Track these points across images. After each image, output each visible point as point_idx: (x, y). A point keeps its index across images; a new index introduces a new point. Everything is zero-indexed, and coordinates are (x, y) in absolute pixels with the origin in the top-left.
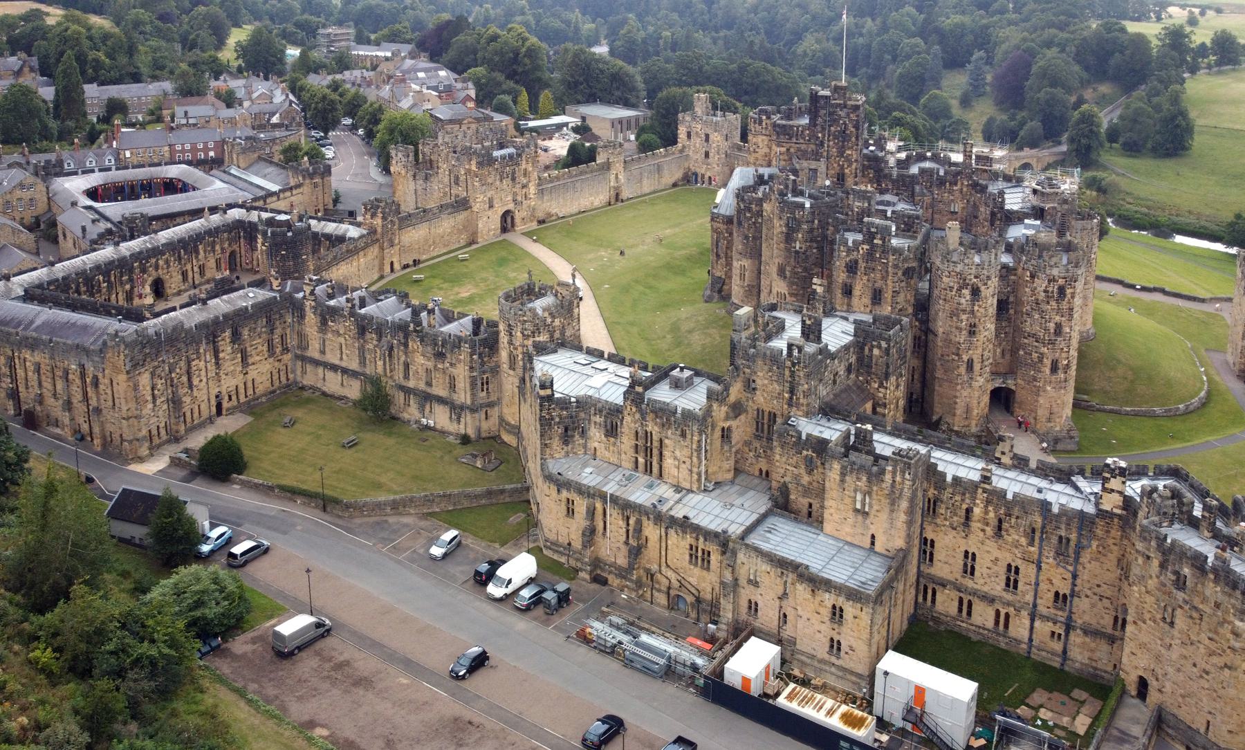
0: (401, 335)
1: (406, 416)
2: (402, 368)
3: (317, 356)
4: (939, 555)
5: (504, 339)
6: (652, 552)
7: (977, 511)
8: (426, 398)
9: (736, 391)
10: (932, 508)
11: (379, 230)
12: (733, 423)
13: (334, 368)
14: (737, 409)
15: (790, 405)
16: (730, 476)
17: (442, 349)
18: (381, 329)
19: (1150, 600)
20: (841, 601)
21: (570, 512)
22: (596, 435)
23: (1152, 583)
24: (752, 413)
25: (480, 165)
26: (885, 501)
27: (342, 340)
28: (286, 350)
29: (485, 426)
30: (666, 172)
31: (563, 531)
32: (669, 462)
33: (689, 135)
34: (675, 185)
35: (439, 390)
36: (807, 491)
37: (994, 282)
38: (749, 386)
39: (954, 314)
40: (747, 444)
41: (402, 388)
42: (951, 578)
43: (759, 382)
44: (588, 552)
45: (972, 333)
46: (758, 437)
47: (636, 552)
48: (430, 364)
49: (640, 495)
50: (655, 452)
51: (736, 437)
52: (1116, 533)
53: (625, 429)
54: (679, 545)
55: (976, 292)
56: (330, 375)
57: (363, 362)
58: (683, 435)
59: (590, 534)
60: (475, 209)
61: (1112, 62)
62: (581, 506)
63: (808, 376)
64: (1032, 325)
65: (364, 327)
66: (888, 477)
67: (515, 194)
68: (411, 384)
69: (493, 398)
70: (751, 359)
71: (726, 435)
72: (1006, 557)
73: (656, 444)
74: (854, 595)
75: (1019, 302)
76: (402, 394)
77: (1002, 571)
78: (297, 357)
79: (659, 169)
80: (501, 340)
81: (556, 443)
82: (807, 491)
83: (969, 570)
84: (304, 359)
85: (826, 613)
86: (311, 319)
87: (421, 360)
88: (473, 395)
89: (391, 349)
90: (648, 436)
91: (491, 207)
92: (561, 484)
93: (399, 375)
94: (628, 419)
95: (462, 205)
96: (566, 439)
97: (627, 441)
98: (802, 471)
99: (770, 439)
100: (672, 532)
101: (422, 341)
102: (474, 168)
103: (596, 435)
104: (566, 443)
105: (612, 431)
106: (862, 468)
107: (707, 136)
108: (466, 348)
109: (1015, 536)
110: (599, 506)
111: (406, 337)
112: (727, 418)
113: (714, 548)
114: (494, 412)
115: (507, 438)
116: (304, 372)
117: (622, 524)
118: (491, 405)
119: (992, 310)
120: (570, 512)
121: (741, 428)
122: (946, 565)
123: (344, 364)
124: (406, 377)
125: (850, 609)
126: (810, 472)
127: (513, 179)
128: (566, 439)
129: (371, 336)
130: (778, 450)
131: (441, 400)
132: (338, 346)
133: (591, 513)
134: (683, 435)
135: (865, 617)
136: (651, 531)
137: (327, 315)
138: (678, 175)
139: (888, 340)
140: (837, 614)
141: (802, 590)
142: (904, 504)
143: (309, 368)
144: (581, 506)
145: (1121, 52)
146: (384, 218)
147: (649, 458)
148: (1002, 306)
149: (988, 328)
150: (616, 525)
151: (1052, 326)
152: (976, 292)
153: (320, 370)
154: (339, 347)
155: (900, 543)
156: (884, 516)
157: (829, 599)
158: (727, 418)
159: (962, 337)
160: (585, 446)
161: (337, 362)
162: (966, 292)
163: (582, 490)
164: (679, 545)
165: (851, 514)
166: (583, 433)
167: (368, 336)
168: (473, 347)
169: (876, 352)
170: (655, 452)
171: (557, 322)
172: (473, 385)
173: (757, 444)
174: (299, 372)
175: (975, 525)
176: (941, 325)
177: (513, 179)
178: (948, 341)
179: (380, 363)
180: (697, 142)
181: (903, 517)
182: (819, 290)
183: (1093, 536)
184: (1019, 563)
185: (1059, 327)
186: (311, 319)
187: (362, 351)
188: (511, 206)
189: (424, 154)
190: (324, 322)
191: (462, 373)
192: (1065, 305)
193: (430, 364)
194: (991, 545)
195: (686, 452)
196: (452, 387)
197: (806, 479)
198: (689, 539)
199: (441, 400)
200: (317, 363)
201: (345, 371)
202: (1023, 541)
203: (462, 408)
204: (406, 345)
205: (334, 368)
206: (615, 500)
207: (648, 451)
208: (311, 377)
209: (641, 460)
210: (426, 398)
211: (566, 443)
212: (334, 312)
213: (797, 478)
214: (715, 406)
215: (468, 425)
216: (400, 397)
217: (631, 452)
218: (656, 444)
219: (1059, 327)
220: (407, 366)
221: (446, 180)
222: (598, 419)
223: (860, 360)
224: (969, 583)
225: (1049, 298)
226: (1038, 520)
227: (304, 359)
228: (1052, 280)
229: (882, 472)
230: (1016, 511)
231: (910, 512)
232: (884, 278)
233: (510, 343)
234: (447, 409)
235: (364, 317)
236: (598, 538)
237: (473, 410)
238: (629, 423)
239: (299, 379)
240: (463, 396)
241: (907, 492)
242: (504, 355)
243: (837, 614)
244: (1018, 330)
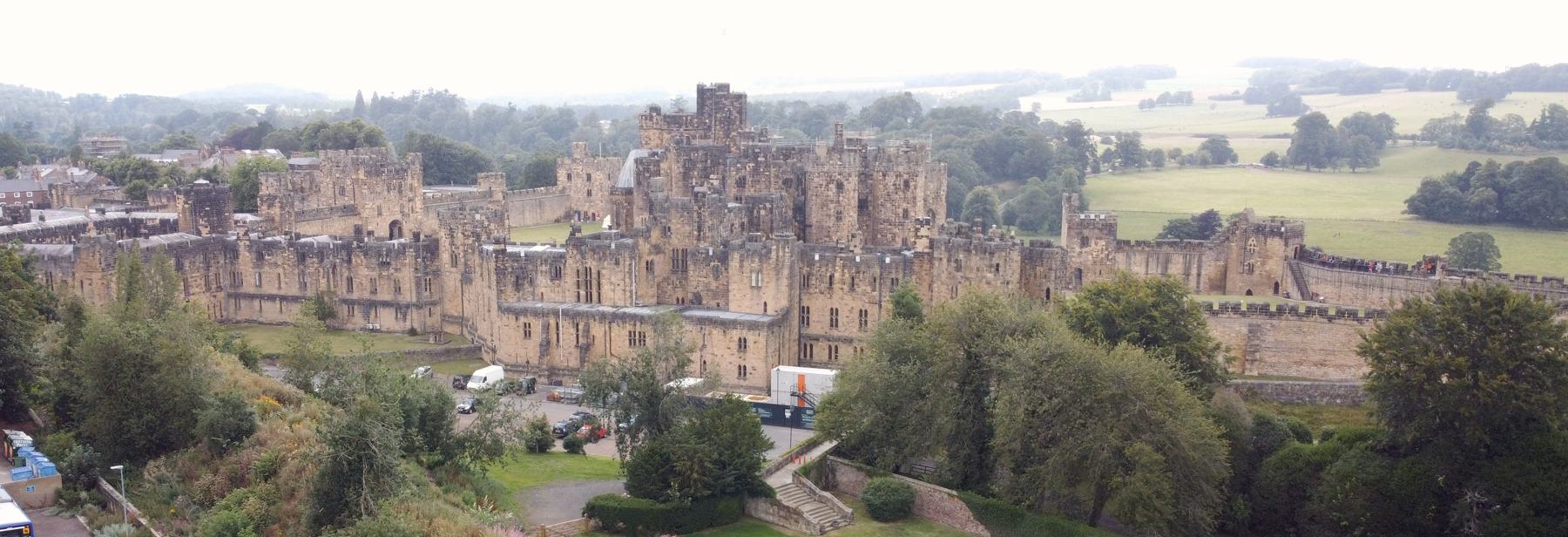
0: (344, 253)
1: (350, 326)
2: (345, 283)
3: (252, 290)
4: (813, 317)
5: (445, 242)
6: (598, 348)
7: (837, 275)
8: (371, 306)
9: (655, 235)
10: (805, 283)
11: (277, 219)
12: (657, 259)
13: (272, 298)
14: (657, 249)
15: (699, 240)
16: (654, 300)
17: (384, 258)
18: (321, 252)
19: (943, 288)
20: (745, 333)
21: (527, 334)
22: (543, 281)
23: (944, 276)
24: (669, 253)
25: (368, 173)
26: (772, 273)
27: (280, 270)
28: (219, 288)
29: (429, 321)
30: (547, 208)
31: (522, 352)
32: (606, 288)
33: (569, 177)
34: (557, 221)
35: (385, 295)
36: (715, 295)
37: (854, 180)
38: (666, 231)
39: (824, 205)
40: (666, 279)
41: (345, 301)
42: (822, 332)
43: (673, 228)
44: (546, 359)
45: (839, 219)
46: (674, 272)
47: (585, 349)
48: (375, 274)
49: (584, 307)
50: (594, 283)
51: (657, 269)
52: (926, 266)
53: (568, 271)
54: (620, 334)
55: (840, 186)
56: (267, 305)
57: (304, 286)
58: (617, 263)
59: (546, 346)
60: (364, 215)
61: (1012, 161)
62: (537, 325)
63: (711, 214)
64: (886, 213)
65: (303, 254)
66: (773, 254)
67: (402, 206)
68: (355, 296)
69: (436, 298)
70: (666, 211)
71: (649, 266)
72: (858, 305)
73: (594, 276)
74: (753, 326)
75: (876, 198)
76: (345, 307)
77: (856, 315)
78: (229, 295)
79: (541, 204)
80: (442, 249)
81: (510, 289)
82: (715, 295)
83: (834, 323)
84: (237, 297)
85: (734, 346)
86: (246, 257)
87: (364, 271)
88: (418, 293)
89: (334, 267)
90: (588, 271)
91: (380, 214)
92: (517, 313)
93: (342, 291)
94: (570, 261)
95: (350, 211)
96: (518, 286)
97: (569, 280)
98: (711, 279)
99: (685, 270)
100: (614, 325)
101: (366, 255)
102: (362, 176)
103: (543, 281)
104: (518, 290)
105: (557, 275)
106: (755, 251)
107: (589, 177)
108: (411, 252)
109: (863, 287)
110: (552, 322)
111: (349, 255)
112: (650, 253)
113: (648, 330)
114: (437, 310)
115: (449, 329)
116: (238, 307)
117: (573, 331)
118: (434, 304)
119: (855, 202)
120: (527, 334)
121: (662, 265)
122: (819, 325)
123: (282, 292)
124: (350, 289)
125: (751, 337)
126: (717, 278)
127: (400, 192)
128: (518, 286)
129: (313, 263)
130: (691, 267)
131: (385, 304)
132: (275, 276)
133: (546, 328)
134: (617, 263)
135: (762, 340)
136: (597, 330)
137: (262, 251)
138: (561, 213)
139: (772, 202)
140: (742, 344)
141: (717, 333)
142: (786, 272)
143: (243, 303)
144: (537, 325)
145: (1021, 152)
146: (282, 208)
147: (589, 285)
148: (863, 205)
149: (852, 216)
150: (567, 333)
151: (900, 211)
152: (840, 186)
153: (256, 303)
154: (279, 277)
155: (784, 303)
156: (772, 285)
157: (735, 334)
158: (650, 253)
159: (831, 222)
160: (533, 293)
161: (274, 291)
162: (832, 186)
163: (536, 313)
164: (620, 334)
165: (748, 290)
166: (531, 282)
167: (308, 261)
168: (417, 251)
169: (763, 212)
170: (594, 283)
171: (492, 226)
172: (418, 284)
173: (674, 278)
174: (232, 308)
175: (836, 286)
176: (814, 216)
177: (400, 192)
178: (821, 228)
179: (323, 281)
180: (579, 183)
181: (785, 282)
182: (716, 183)
183: (912, 272)
184: (867, 306)
185: (906, 212)
186: (246, 257)
187: (302, 274)
188: (398, 217)
189: (293, 183)
190: (260, 257)
191: (407, 276)
192: (909, 194)
193: (375, 274)
194: (848, 299)
195: (620, 276)
196: (398, 290)
197: (714, 285)
198: (629, 327)
199: (385, 304)
200: (252, 297)
201: (283, 298)
202: (869, 289)
203: (408, 306)
204: (349, 261)
205: (272, 298)
206: (566, 313)
207: (588, 284)
208: (247, 310)
209: (583, 293)
210: (371, 306)
211: (518, 290)
212: (272, 246)
213: (707, 285)
214: (641, 241)
215: (415, 319)
216: (343, 311)
217: (574, 288)
218: (594, 276)
219: (906, 212)
220: (350, 280)
221: (330, 193)
222: (544, 268)
223: (751, 222)
224: (835, 333)
225: (897, 189)
226: (877, 270)
227: (237, 297)
228: (899, 175)
229: (770, 251)
230: (863, 268)
231: (791, 286)
232: (768, 187)
233: (452, 244)
234: (393, 311)
235: (305, 245)
236: (553, 350)
237: (419, 306)
238: (571, 265)
239: (232, 316)
240: (409, 296)
241: (787, 263)
242: (445, 256)
243: (742, 344)
244: (876, 221)
